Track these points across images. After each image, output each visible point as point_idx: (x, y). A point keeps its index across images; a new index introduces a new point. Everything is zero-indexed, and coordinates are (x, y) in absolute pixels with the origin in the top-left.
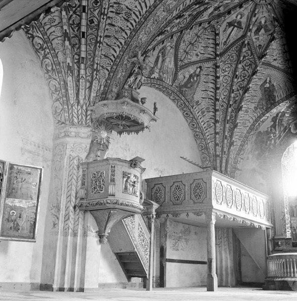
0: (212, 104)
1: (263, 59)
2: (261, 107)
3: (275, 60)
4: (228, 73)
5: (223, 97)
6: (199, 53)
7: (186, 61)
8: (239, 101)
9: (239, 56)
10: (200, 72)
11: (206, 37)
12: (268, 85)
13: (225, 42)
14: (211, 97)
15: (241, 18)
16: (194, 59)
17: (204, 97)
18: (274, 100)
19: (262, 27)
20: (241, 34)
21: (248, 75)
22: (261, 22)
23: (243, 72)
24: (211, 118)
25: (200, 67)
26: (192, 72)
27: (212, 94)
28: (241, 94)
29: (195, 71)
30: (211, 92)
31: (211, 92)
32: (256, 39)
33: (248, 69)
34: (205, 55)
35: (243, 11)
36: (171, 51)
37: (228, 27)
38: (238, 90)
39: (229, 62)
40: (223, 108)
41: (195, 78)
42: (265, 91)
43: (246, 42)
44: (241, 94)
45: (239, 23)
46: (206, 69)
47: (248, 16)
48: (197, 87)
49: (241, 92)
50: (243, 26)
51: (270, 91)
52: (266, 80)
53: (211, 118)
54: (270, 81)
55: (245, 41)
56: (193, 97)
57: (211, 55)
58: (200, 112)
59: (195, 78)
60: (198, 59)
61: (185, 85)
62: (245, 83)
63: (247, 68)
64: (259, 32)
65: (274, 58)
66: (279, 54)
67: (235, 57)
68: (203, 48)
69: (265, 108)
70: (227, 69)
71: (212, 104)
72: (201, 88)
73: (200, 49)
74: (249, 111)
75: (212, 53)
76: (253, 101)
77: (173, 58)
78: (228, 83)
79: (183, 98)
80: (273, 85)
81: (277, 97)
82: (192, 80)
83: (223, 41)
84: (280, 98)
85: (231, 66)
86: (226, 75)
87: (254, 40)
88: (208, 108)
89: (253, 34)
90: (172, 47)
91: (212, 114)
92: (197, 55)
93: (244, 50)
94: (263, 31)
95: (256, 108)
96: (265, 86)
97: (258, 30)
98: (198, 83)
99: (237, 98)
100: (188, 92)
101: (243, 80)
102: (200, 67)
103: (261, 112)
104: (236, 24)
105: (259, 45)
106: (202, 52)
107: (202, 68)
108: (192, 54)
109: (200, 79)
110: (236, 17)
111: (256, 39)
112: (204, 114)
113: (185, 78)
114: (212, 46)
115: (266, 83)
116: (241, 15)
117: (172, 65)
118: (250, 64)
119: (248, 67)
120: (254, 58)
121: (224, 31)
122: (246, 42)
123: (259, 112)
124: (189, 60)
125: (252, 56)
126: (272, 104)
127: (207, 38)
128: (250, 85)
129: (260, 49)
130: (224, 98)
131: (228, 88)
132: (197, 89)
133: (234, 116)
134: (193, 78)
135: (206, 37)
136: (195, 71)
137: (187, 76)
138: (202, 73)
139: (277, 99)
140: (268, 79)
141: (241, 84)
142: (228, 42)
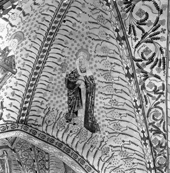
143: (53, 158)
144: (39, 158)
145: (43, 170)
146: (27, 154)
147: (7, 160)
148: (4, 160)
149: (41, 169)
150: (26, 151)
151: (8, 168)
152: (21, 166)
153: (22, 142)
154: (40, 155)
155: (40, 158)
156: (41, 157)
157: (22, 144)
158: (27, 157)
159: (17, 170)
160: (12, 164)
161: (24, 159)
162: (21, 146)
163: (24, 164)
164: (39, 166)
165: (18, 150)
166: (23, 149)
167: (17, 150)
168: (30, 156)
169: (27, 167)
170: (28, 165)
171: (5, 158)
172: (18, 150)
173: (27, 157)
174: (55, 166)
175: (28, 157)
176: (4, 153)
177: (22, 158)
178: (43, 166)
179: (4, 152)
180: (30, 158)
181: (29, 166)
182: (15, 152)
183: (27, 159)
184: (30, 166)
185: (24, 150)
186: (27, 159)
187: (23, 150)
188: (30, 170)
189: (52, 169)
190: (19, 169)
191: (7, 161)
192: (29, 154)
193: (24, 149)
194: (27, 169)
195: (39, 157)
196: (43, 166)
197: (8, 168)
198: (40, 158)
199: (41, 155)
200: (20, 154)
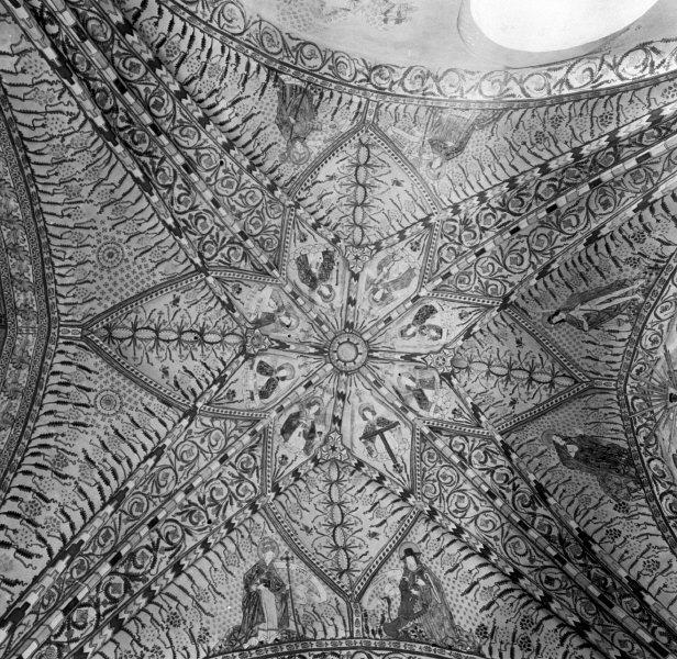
0: (523, 600)
1: (483, 418)
2: (625, 491)
3: (513, 403)
4: (476, 508)
5: (524, 561)
6: (373, 530)
7: (360, 566)
8: (565, 532)
9: (451, 465)
10: (417, 562)
11: (353, 492)
12: (573, 449)
13: (396, 466)
14: (503, 587)
15: (374, 413)
16: (375, 547)
17: (486, 603)
18: (621, 452)
19: (420, 390)
20: (406, 432)
21: (506, 471)
22: (408, 388)
23: (495, 476)
24: (563, 640)
25: (409, 552)
26: (398, 575)
27: (497, 578)
28: (548, 514)
29: (406, 568)
30: (487, 576)
31: (487, 576)
32: (436, 412)
33: (494, 462)
34: (390, 521)
35: (360, 400)
36: (293, 567)
37: (370, 444)
38: (534, 515)
39: (450, 489)
40: (557, 584)
41: (421, 582)
42: (586, 461)
43: (426, 431)
44: (548, 514)
45: (382, 421)
46: (423, 544)
47: (377, 399)
48: (443, 598)
49: (541, 510)
50: (393, 418)
51: (591, 450)
52: (557, 445)
53: (563, 640)
54: (565, 439)
55: (422, 434)
56: (454, 627)
57: (401, 509)
58: (516, 647)
59: (421, 582)
60: (383, 540)
61: (406, 614)
62: (523, 486)
63: (489, 464)
64: (426, 399)
65: (508, 401)
66: (505, 389)
67: (449, 473)
68: (370, 515)
69: (632, 485)
70: (463, 505)
71: (523, 600)
72: (455, 591)
73: (368, 522)
74: (618, 527)
75: (397, 505)
76: (595, 501)
77: (315, 580)
78: (498, 525)
79: (417, 647)
80: (582, 437)
81: (615, 442)
82: (414, 592)
83: (391, 469)
84: (623, 436)
85: (462, 491)
86: (477, 516)
87: (437, 416)
88: (526, 622)
89: (422, 412)
90: (287, 559)
91: (551, 624)
92: (373, 535)
93: (440, 444)
94: (428, 393)
95: (621, 506)
96: (573, 455)
97: (422, 399)
98: (438, 586)
99: (555, 532)
100: (430, 624)
101: (514, 488)
102: (409, 552)
103: (643, 501)
104: (378, 428)
105: (453, 413)
106: (378, 521)
107: (415, 551)
108: (357, 542)
109: (431, 574)
110: (365, 418)
111: (436, 412)
112: (534, 644)
113: (389, 602)
114: (381, 494)
115: (564, 447)
116: (368, 409)
117: (324, 593)
118: (484, 452)
119: (489, 460)
120: (473, 435)
121: (370, 453)
122: (426, 431)
123: (638, 504)
124: (365, 558)
125: (470, 439)
126: (629, 462)
127: (359, 491)
128: (532, 477)
129: (460, 415)
130: (532, 560)
131: (512, 533)
132: (448, 599)
133: (602, 574)
134: (415, 586)
135: (353, 492)
136: (406, 568)
137: (394, 593)
138: (424, 560)
139: (623, 444)
140: (558, 440)
141: (521, 498)
142: (400, 462)
143: (474, 183)
144: (504, 221)
145: (540, 192)
146: (514, 256)
147: (583, 307)
148: (587, 316)
149: (542, 199)
150: (504, 261)
151: (609, 296)
152: (554, 261)
153: (477, 284)
154: (493, 221)
155: (504, 216)
156: (499, 217)
157: (484, 280)
158: (526, 255)
159: (597, 268)
160: (587, 289)
161: (534, 259)
162: (491, 282)
163: (552, 253)
164: (534, 207)
165: (507, 285)
166: (499, 274)
167: (509, 290)
168: (519, 247)
169: (558, 243)
170: (550, 241)
171: (578, 313)
172: (507, 285)
173: (526, 255)
174: (498, 167)
175: (524, 250)
176: (563, 320)
177: (534, 267)
178: (524, 197)
179: (560, 322)
180: (525, 245)
181: (554, 237)
182: (512, 292)
183: (533, 252)
184: (551, 233)
185: (504, 270)
186: (533, 252)
187: (505, 272)
188: (566, 230)
189: (513, 166)
190: (585, 260)
191: (586, 306)
192: (509, 252)
193: (500, 270)
194: (564, 239)
195: (500, 221)
196: (524, 197)
197: (609, 296)
198: (504, 216)
199: (490, 217)
200: (520, 277)
